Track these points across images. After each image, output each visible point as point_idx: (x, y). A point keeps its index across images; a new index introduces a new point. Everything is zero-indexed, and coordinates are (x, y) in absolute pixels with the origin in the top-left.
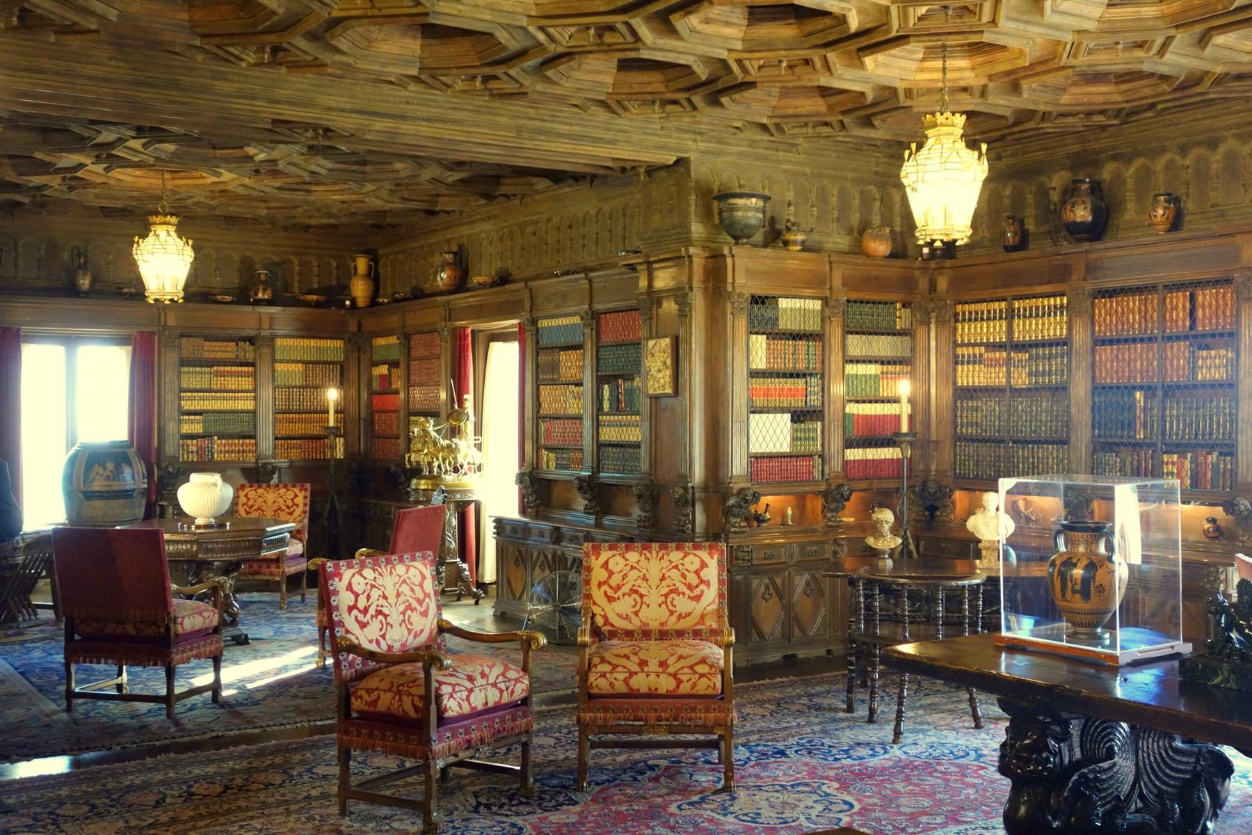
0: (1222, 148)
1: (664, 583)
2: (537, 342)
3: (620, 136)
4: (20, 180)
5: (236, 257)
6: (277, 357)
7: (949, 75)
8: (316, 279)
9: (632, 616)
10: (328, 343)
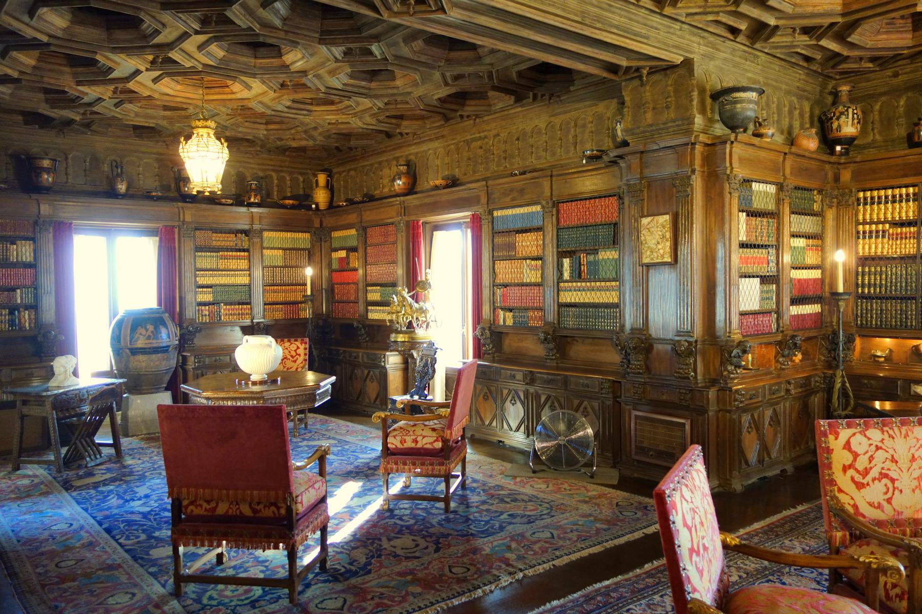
1: (915, 465)
2: (493, 228)
6: (265, 245)
8: (289, 190)
9: (885, 504)
10: (300, 235)
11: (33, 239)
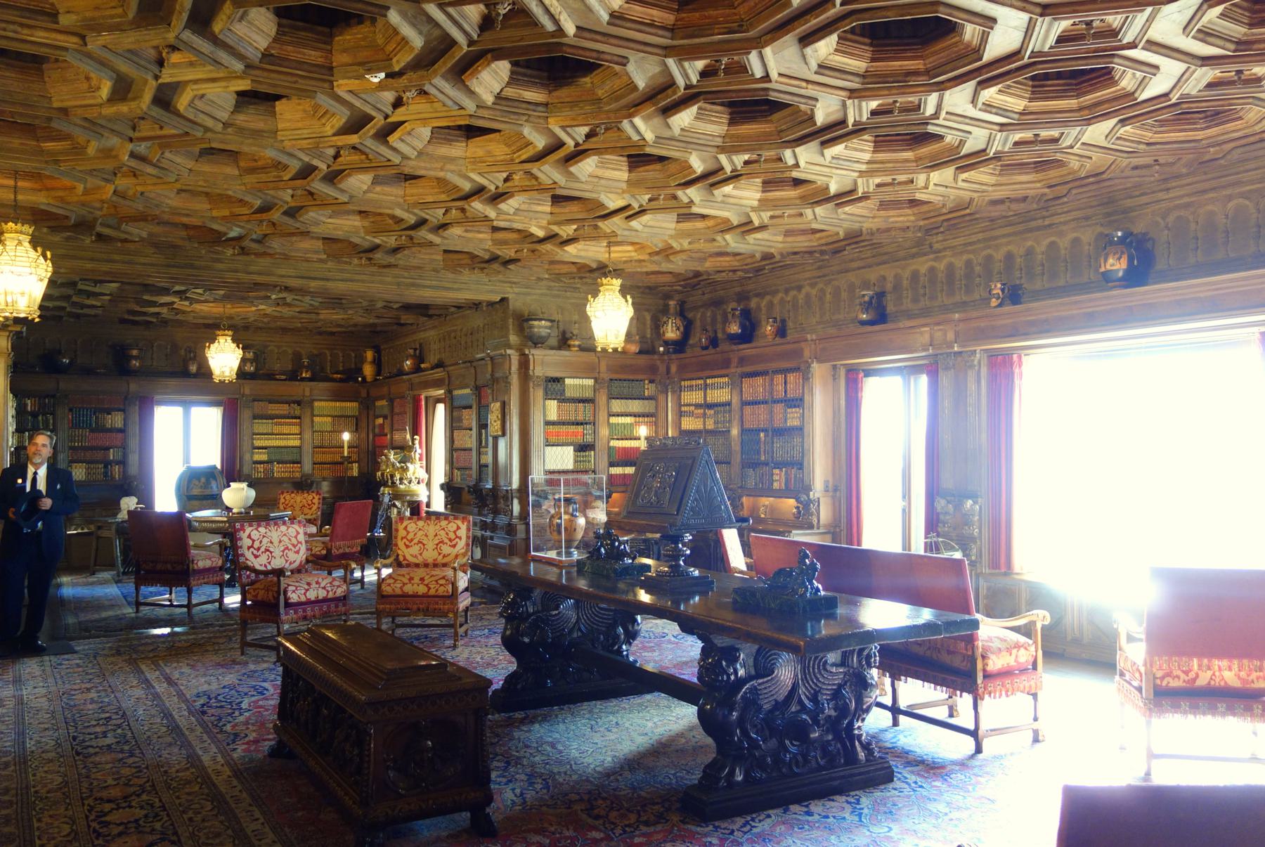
0: (804, 291)
3: (463, 286)
4: (144, 310)
5: (290, 351)
7: (612, 255)
10: (348, 404)
11: (124, 411)
